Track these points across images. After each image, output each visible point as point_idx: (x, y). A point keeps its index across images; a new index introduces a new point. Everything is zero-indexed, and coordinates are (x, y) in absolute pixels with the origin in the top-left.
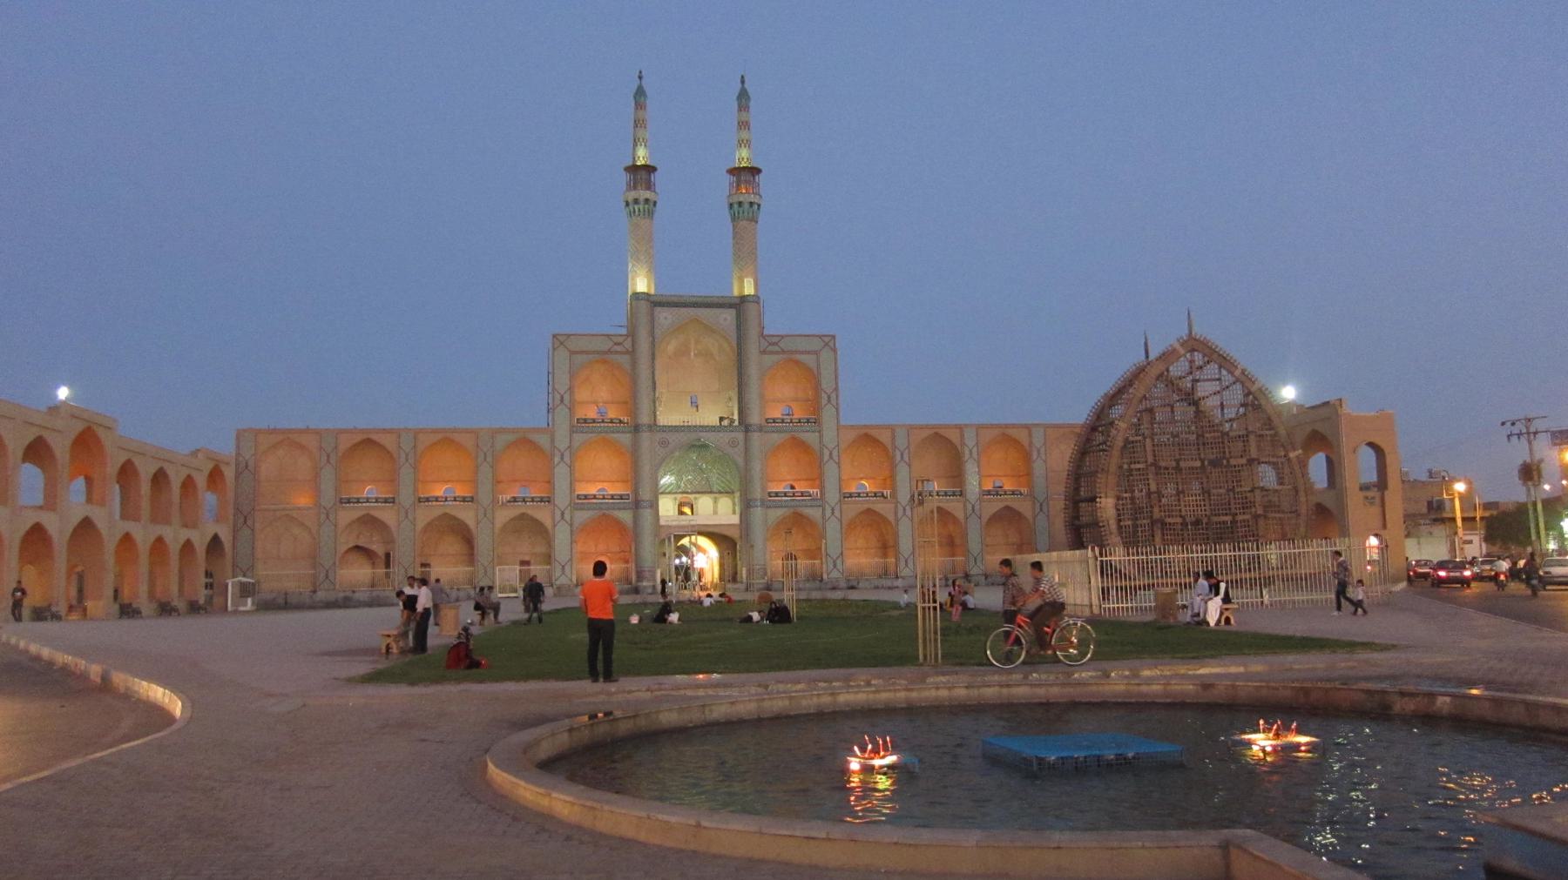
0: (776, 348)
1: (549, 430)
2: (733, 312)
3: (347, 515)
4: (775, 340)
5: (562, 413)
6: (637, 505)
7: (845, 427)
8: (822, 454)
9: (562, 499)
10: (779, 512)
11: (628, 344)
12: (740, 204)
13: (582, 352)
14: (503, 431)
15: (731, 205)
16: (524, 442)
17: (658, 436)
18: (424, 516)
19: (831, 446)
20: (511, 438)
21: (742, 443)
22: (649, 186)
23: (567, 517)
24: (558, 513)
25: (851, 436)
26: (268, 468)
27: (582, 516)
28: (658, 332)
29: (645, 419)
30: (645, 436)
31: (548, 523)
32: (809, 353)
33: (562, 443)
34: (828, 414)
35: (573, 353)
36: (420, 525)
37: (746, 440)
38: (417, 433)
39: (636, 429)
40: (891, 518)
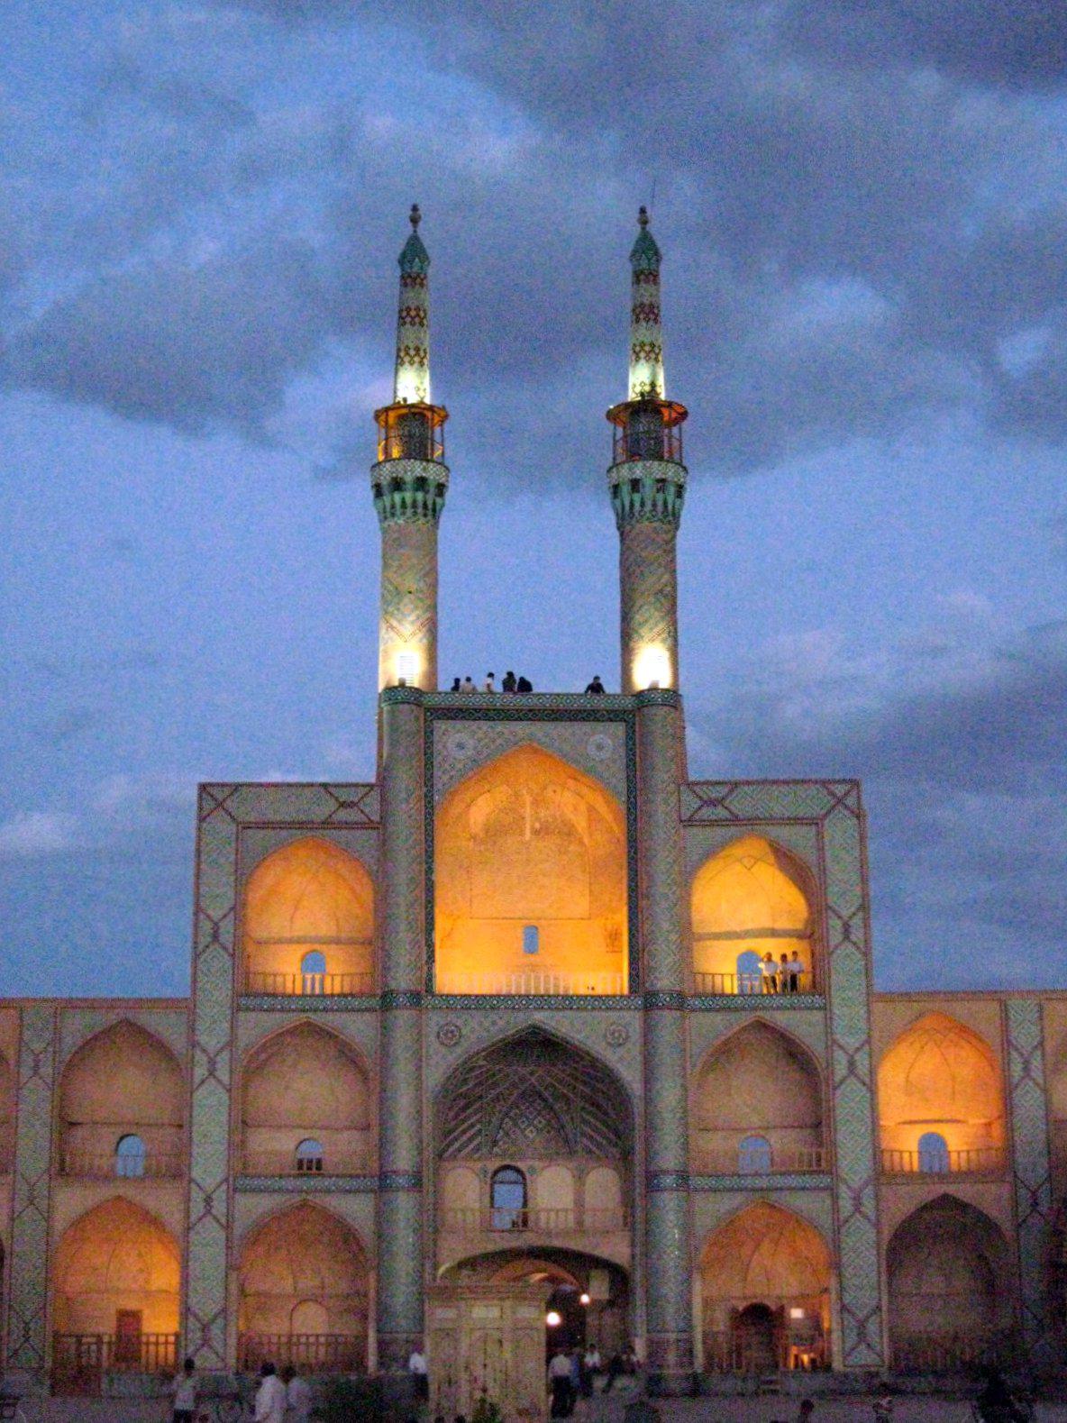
0: (720, 812)
1: (187, 1008)
2: (619, 729)
4: (715, 793)
5: (219, 961)
7: (889, 997)
8: (830, 1065)
11: (372, 807)
12: (635, 484)
13: (263, 825)
14: (71, 1004)
15: (616, 489)
19: (852, 1042)
23: (219, 1208)
24: (198, 1197)
28: (441, 778)
32: (798, 821)
33: (212, 1038)
35: (247, 826)
39: (386, 1001)
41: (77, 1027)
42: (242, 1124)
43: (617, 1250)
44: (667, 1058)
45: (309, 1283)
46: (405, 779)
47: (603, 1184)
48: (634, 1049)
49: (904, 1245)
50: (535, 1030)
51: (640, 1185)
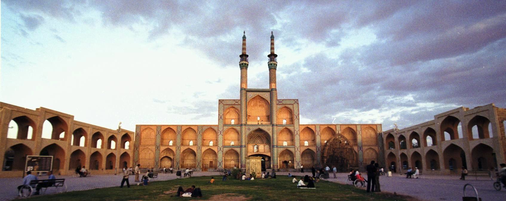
3: (162, 148)
5: (221, 120)
6: (241, 147)
9: (220, 144)
10: (282, 149)
12: (271, 64)
16: (211, 128)
17: (247, 127)
18: (183, 148)
20: (206, 128)
21: (271, 129)
22: (246, 61)
23: (222, 149)
25: (303, 127)
26: (144, 135)
27: (226, 149)
28: (248, 99)
29: (244, 122)
30: (244, 127)
31: (216, 152)
34: (296, 122)
36: (182, 151)
37: (273, 129)
38: (182, 126)
39: (241, 125)
40: (315, 151)
41: (204, 128)
42: (224, 140)
43: (269, 154)
44: (275, 132)
45: (232, 158)
46: (244, 99)
47: (267, 146)
48: (271, 130)
49: (303, 154)
50: (259, 128)
51: (271, 147)
